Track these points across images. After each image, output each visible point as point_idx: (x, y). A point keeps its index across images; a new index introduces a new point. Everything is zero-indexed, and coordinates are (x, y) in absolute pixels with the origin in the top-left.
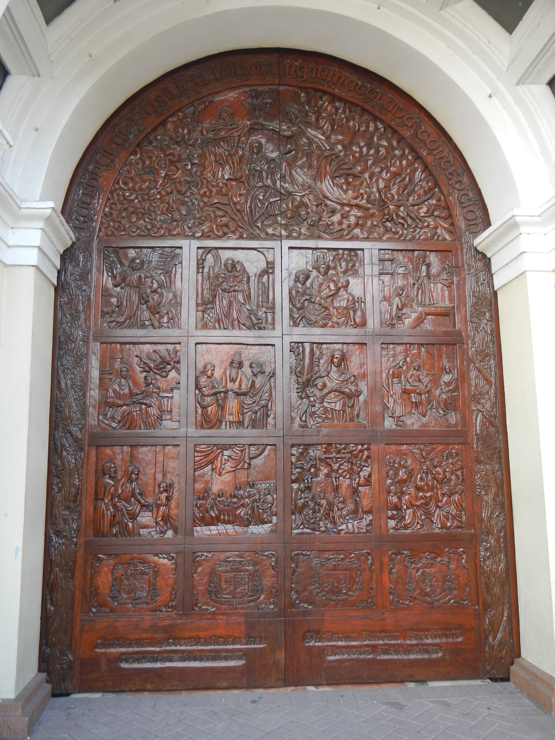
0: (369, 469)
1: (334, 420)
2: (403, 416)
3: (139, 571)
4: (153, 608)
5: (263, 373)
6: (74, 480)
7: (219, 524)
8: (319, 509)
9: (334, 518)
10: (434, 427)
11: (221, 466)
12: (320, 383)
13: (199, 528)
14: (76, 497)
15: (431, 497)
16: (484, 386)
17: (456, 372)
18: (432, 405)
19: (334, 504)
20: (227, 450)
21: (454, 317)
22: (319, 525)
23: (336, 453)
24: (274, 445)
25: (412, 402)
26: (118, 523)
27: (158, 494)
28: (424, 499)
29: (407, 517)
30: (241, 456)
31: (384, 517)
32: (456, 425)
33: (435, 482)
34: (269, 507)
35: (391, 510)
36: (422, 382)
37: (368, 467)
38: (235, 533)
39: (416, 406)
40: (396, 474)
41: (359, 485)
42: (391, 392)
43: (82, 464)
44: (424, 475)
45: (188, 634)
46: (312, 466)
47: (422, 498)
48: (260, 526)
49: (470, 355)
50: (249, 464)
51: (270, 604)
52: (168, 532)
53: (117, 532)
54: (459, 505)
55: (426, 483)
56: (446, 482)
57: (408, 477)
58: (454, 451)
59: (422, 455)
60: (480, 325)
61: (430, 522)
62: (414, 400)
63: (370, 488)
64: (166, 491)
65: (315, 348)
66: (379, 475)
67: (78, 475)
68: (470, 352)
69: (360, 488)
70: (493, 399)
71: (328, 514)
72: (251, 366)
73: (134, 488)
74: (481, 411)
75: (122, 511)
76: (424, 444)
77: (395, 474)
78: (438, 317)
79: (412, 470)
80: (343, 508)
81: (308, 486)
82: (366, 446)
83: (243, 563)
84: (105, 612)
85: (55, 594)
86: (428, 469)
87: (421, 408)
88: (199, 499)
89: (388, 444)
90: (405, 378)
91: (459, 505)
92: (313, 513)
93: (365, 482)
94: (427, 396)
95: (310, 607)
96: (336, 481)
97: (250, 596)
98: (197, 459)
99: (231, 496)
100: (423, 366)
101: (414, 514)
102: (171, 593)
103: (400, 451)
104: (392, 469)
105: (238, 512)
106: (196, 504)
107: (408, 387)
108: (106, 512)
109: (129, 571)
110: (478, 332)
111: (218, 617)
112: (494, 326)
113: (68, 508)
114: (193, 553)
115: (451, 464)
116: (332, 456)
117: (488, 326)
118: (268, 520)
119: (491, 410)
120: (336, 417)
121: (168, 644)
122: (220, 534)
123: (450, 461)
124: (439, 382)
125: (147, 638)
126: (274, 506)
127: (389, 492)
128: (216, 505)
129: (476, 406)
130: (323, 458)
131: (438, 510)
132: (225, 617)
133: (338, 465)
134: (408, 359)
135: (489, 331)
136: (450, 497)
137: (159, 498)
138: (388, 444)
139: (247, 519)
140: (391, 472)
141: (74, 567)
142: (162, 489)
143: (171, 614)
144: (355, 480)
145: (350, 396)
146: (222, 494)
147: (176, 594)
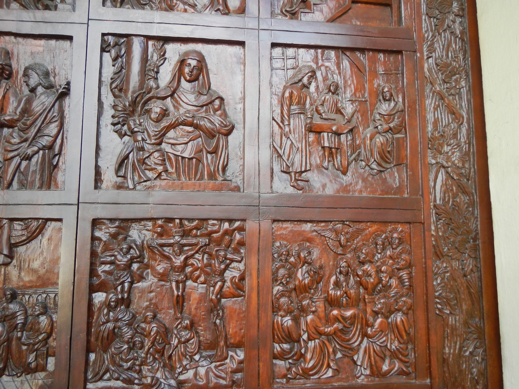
0: (241, 266)
1: (179, 176)
2: (306, 171)
5: (50, 87)
8: (142, 343)
9: (170, 357)
10: (361, 191)
12: (156, 108)
15: (354, 317)
16: (449, 124)
17: (401, 100)
18: (359, 155)
19: (173, 333)
21: (399, 7)
22: (140, 372)
23: (182, 237)
25: (323, 148)
28: (340, 321)
29: (309, 356)
31: (266, 356)
32: (400, 189)
33: (362, 291)
34: (40, 341)
35: (280, 342)
36: (342, 113)
37: (240, 262)
39: (331, 154)
40: (291, 275)
41: (221, 294)
42: (287, 129)
44: (342, 278)
46: (131, 261)
47: (336, 319)
49: (426, 70)
54: (404, 334)
55: (346, 293)
56: (380, 291)
57: (312, 281)
58: (395, 235)
59: (340, 241)
60: (443, 21)
61: (351, 363)
62: (326, 144)
63: (242, 301)
65: (150, 49)
66: (258, 277)
68: (426, 66)
69: (223, 300)
70: (465, 147)
71: (161, 352)
72: (26, 75)
74: (444, 167)
76: (343, 222)
77: (290, 276)
78: (373, 6)
79: (321, 267)
80: (188, 340)
81: (123, 298)
82: (237, 224)
86: (349, 266)
87: (339, 158)
89: (278, 221)
90: (311, 105)
91: (404, 334)
92: (130, 349)
93: (233, 290)
94: (349, 138)
96: (178, 288)
100: (345, 87)
101: (322, 350)
103: (301, 233)
104: (283, 266)
107: (317, 121)
110: (440, 34)
112: (466, 25)
115: (391, 257)
116: (172, 241)
117: (457, 25)
118: (37, 365)
119: (460, 165)
120: (184, 171)
123: (388, 253)
124: (371, 114)
127: (276, 309)
129: (434, 158)
130: (154, 244)
131: (365, 339)
133: (182, 258)
134: (318, 74)
135: (458, 32)
136: (387, 318)
138: (278, 221)
140: (282, 272)
144: (214, 287)
145: (211, 134)
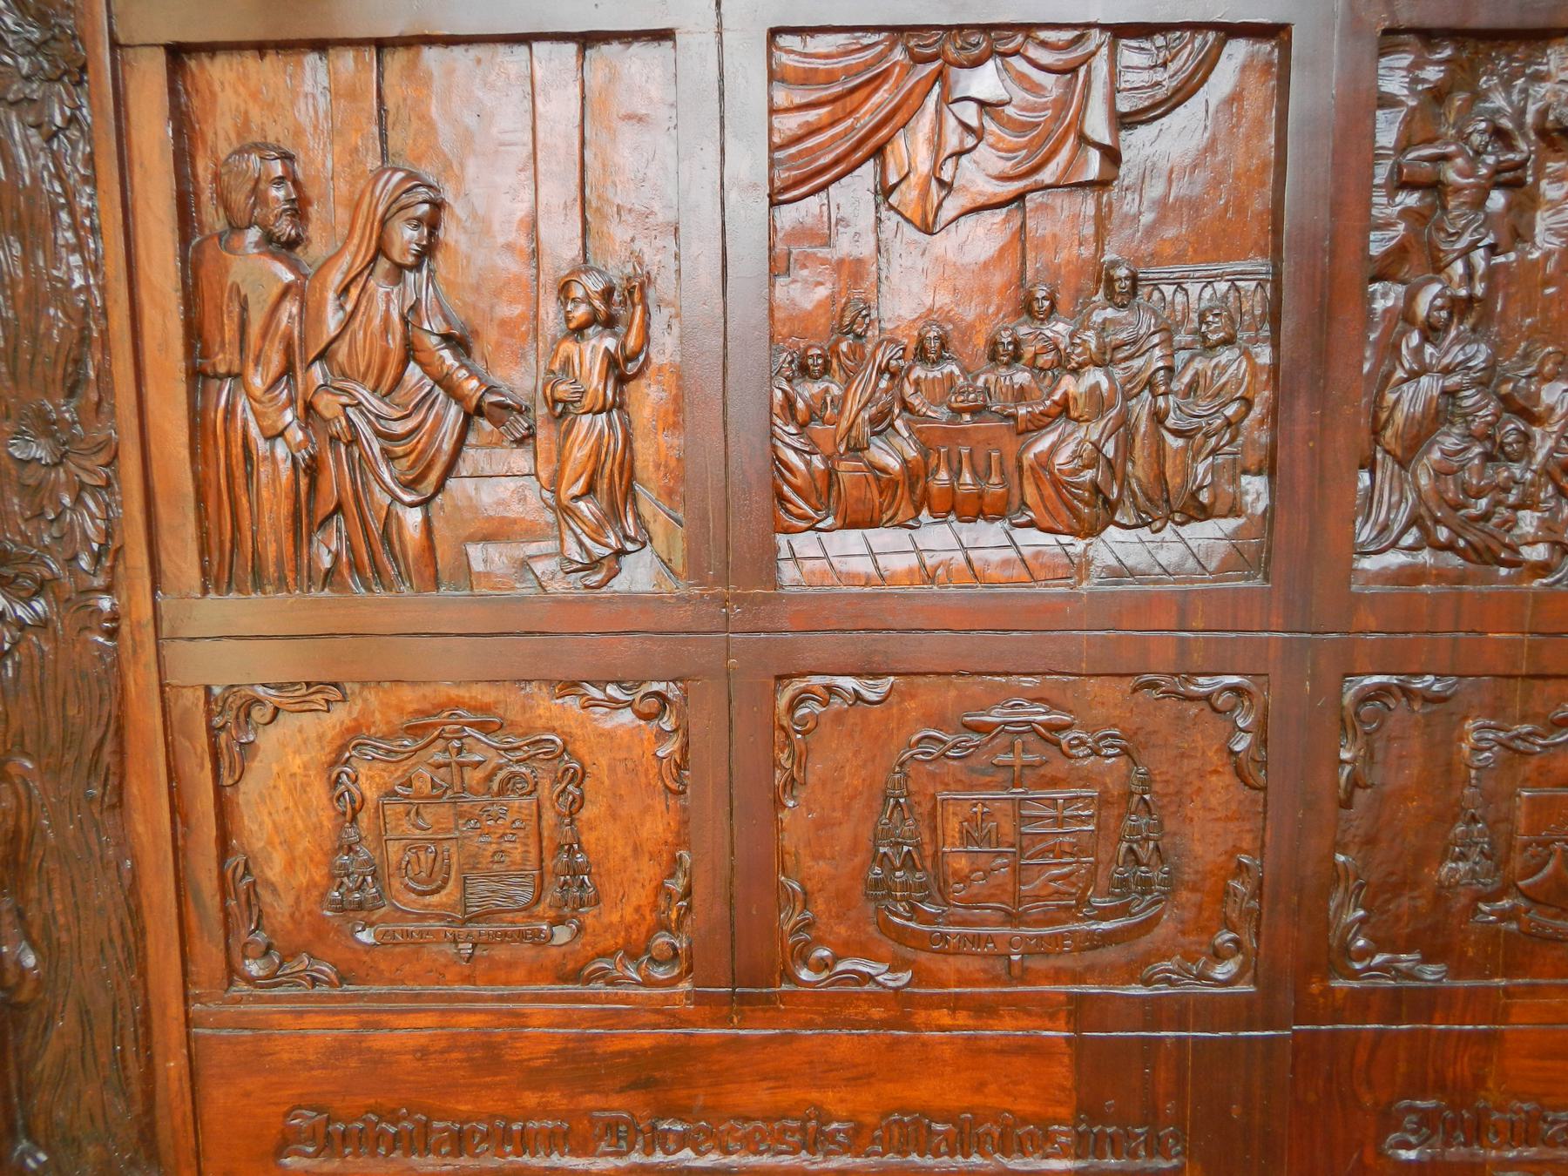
3: (479, 774)
4: (570, 966)
6: (55, 259)
7: (925, 515)
8: (1526, 438)
11: (937, 167)
13: (805, 543)
14: (79, 362)
20: (977, 63)
24: (1274, 32)
26: (339, 508)
27: (556, 342)
30: (1062, 104)
34: (1229, 423)
38: (1018, 572)
43: (90, 160)
45: (762, 1096)
48: (1167, 533)
50: (1112, 156)
51: (1218, 956)
52: (626, 561)
53: (337, 557)
64: (610, 323)
67: (75, 227)
73: (414, 308)
75: (354, 440)
83: (1065, 738)
84: (315, 981)
85: (33, 892)
88: (804, 370)
92: (1488, 457)
95: (1431, 973)
97: (1105, 914)
98: (790, 124)
99: (993, 357)
102: (660, 888)
105: (1044, 444)
106: (789, 402)
108: (261, 446)
109: (426, 773)
111: (921, 1016)
113: (45, 426)
114: (779, 678)
121: (656, 1140)
122: (931, 578)
125: (545, 1112)
126: (1257, 411)
128: (906, 407)
132: (962, 1018)
137: (568, 361)
139: (1096, 489)
141: (121, 751)
142: (581, 312)
143: (667, 999)
146: (944, 344)
147: (688, 893)
